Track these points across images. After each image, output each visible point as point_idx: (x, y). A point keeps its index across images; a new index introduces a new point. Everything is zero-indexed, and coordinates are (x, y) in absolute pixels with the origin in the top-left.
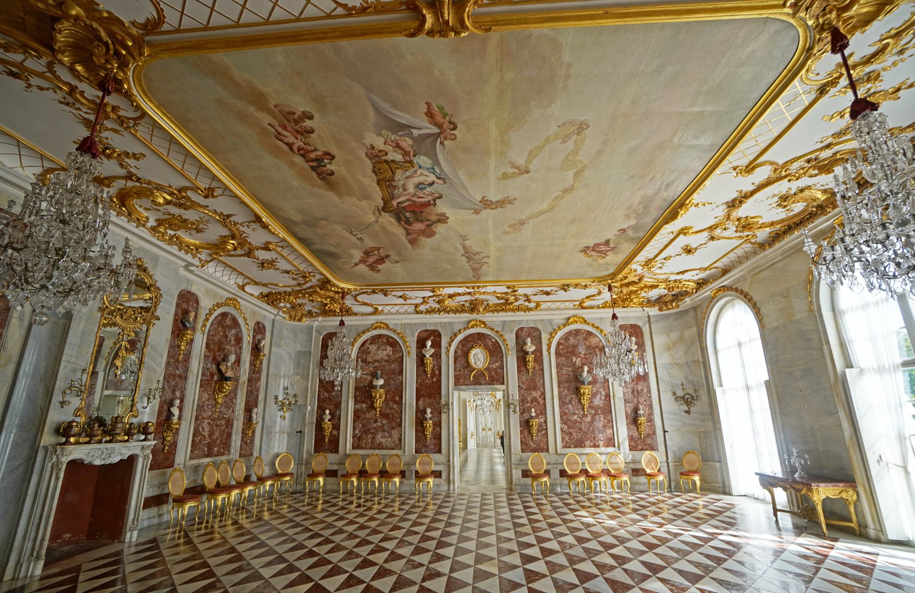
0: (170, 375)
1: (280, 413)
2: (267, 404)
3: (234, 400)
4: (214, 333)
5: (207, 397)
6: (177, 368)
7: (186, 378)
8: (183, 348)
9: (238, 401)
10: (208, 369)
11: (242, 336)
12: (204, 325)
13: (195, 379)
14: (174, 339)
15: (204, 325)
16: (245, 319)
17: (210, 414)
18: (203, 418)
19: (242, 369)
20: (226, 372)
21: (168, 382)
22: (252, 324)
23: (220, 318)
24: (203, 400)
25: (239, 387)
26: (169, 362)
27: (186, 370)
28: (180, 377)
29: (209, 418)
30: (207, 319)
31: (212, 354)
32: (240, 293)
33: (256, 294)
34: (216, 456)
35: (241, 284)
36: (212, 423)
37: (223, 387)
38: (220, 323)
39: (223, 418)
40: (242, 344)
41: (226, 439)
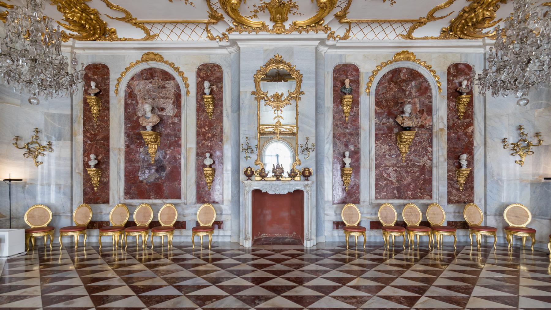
0: (339, 135)
1: (518, 158)
2: (487, 149)
3: (429, 149)
4: (384, 91)
5: (388, 147)
6: (347, 128)
7: (358, 135)
8: (346, 111)
9: (435, 149)
10: (383, 124)
11: (429, 85)
12: (368, 88)
13: (368, 134)
14: (337, 106)
15: (368, 88)
16: (428, 67)
17: (395, 162)
18: (386, 166)
19: (435, 118)
20: (403, 123)
21: (339, 139)
22: (441, 70)
23: (390, 75)
24: (383, 151)
25: (434, 136)
26: (337, 125)
27: (358, 128)
28: (351, 134)
29: (394, 165)
30: (371, 81)
31: (386, 110)
32: (408, 43)
33: (438, 34)
34: (410, 198)
35: (405, 33)
36: (399, 170)
37: (401, 138)
38: (391, 79)
39: (415, 165)
40: (431, 92)
41: (423, 184)
